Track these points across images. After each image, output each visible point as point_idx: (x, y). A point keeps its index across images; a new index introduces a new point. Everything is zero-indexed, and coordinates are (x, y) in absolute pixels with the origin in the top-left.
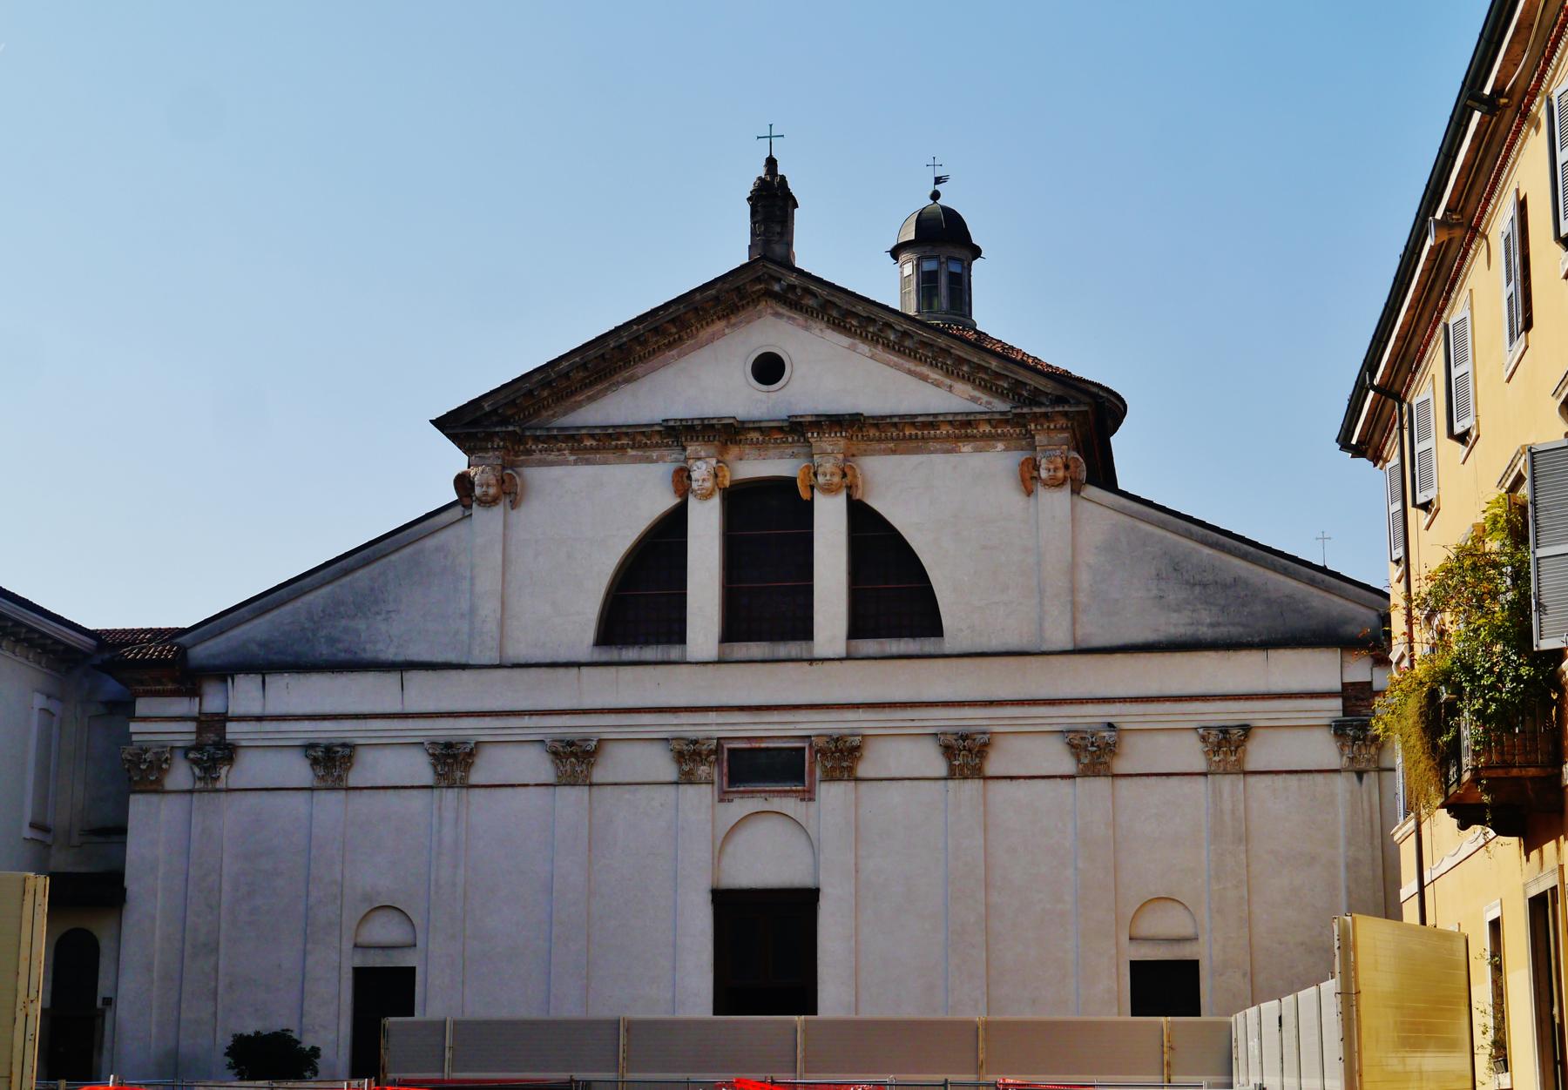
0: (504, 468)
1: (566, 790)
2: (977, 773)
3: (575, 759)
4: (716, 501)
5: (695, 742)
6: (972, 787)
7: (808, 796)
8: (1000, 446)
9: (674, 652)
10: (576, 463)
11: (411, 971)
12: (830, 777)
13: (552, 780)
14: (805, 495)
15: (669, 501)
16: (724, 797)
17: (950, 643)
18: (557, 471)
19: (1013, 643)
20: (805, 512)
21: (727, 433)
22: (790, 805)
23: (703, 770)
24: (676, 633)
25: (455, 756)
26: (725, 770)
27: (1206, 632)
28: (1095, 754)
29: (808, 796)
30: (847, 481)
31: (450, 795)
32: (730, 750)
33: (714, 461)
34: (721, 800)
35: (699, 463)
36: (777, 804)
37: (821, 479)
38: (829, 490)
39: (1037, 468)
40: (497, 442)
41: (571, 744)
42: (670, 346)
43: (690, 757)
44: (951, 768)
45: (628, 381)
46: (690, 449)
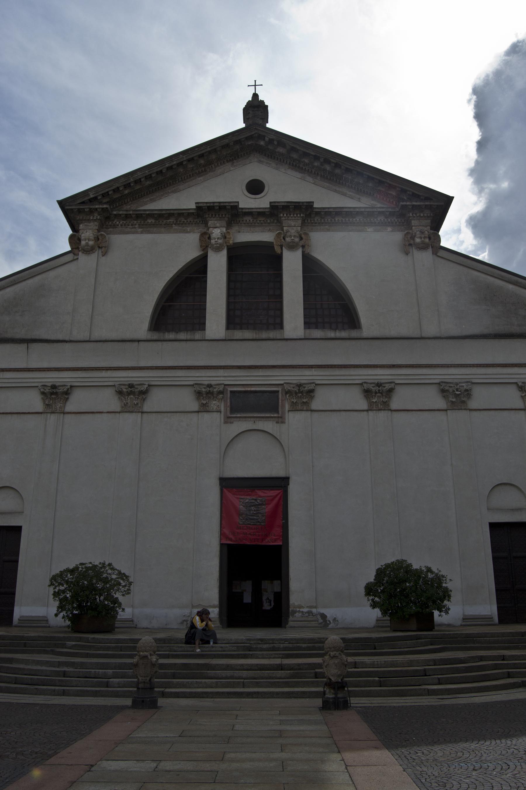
0: (99, 231)
1: (127, 415)
2: (385, 406)
3: (133, 396)
4: (225, 252)
5: (210, 386)
6: (382, 415)
7: (281, 420)
8: (389, 229)
9: (198, 335)
10: (142, 233)
11: (18, 529)
12: (294, 408)
13: (119, 409)
14: (277, 249)
15: (194, 253)
16: (228, 420)
17: (366, 332)
18: (131, 237)
19: (404, 332)
20: (276, 262)
21: (232, 214)
22: (269, 426)
23: (214, 404)
24: (198, 322)
25: (56, 393)
26: (229, 404)
27: (515, 329)
28: (457, 397)
29: (281, 420)
30: (302, 243)
31: (53, 418)
32: (231, 392)
33: (224, 230)
34: (225, 422)
35: (216, 230)
36: (261, 425)
37: (288, 239)
38: (292, 247)
39: (413, 238)
40: (96, 216)
41: (131, 386)
42: (199, 174)
43: (205, 395)
44: (371, 404)
45: (175, 192)
46: (210, 223)
